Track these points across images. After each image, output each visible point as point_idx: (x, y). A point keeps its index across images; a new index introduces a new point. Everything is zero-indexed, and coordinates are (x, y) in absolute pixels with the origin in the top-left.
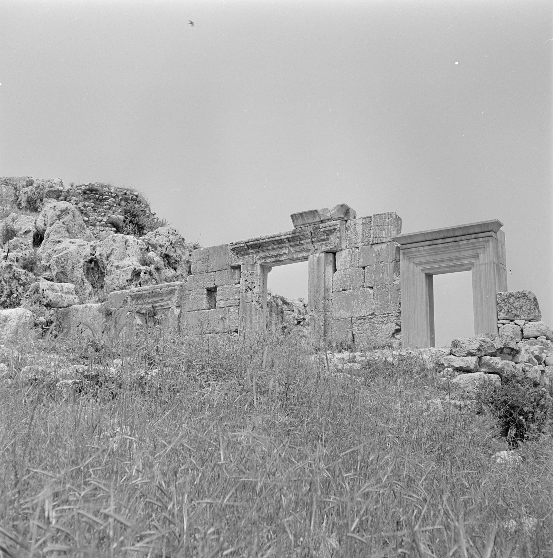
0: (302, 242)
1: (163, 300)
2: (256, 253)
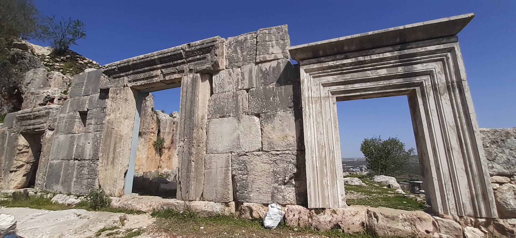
0: (176, 62)
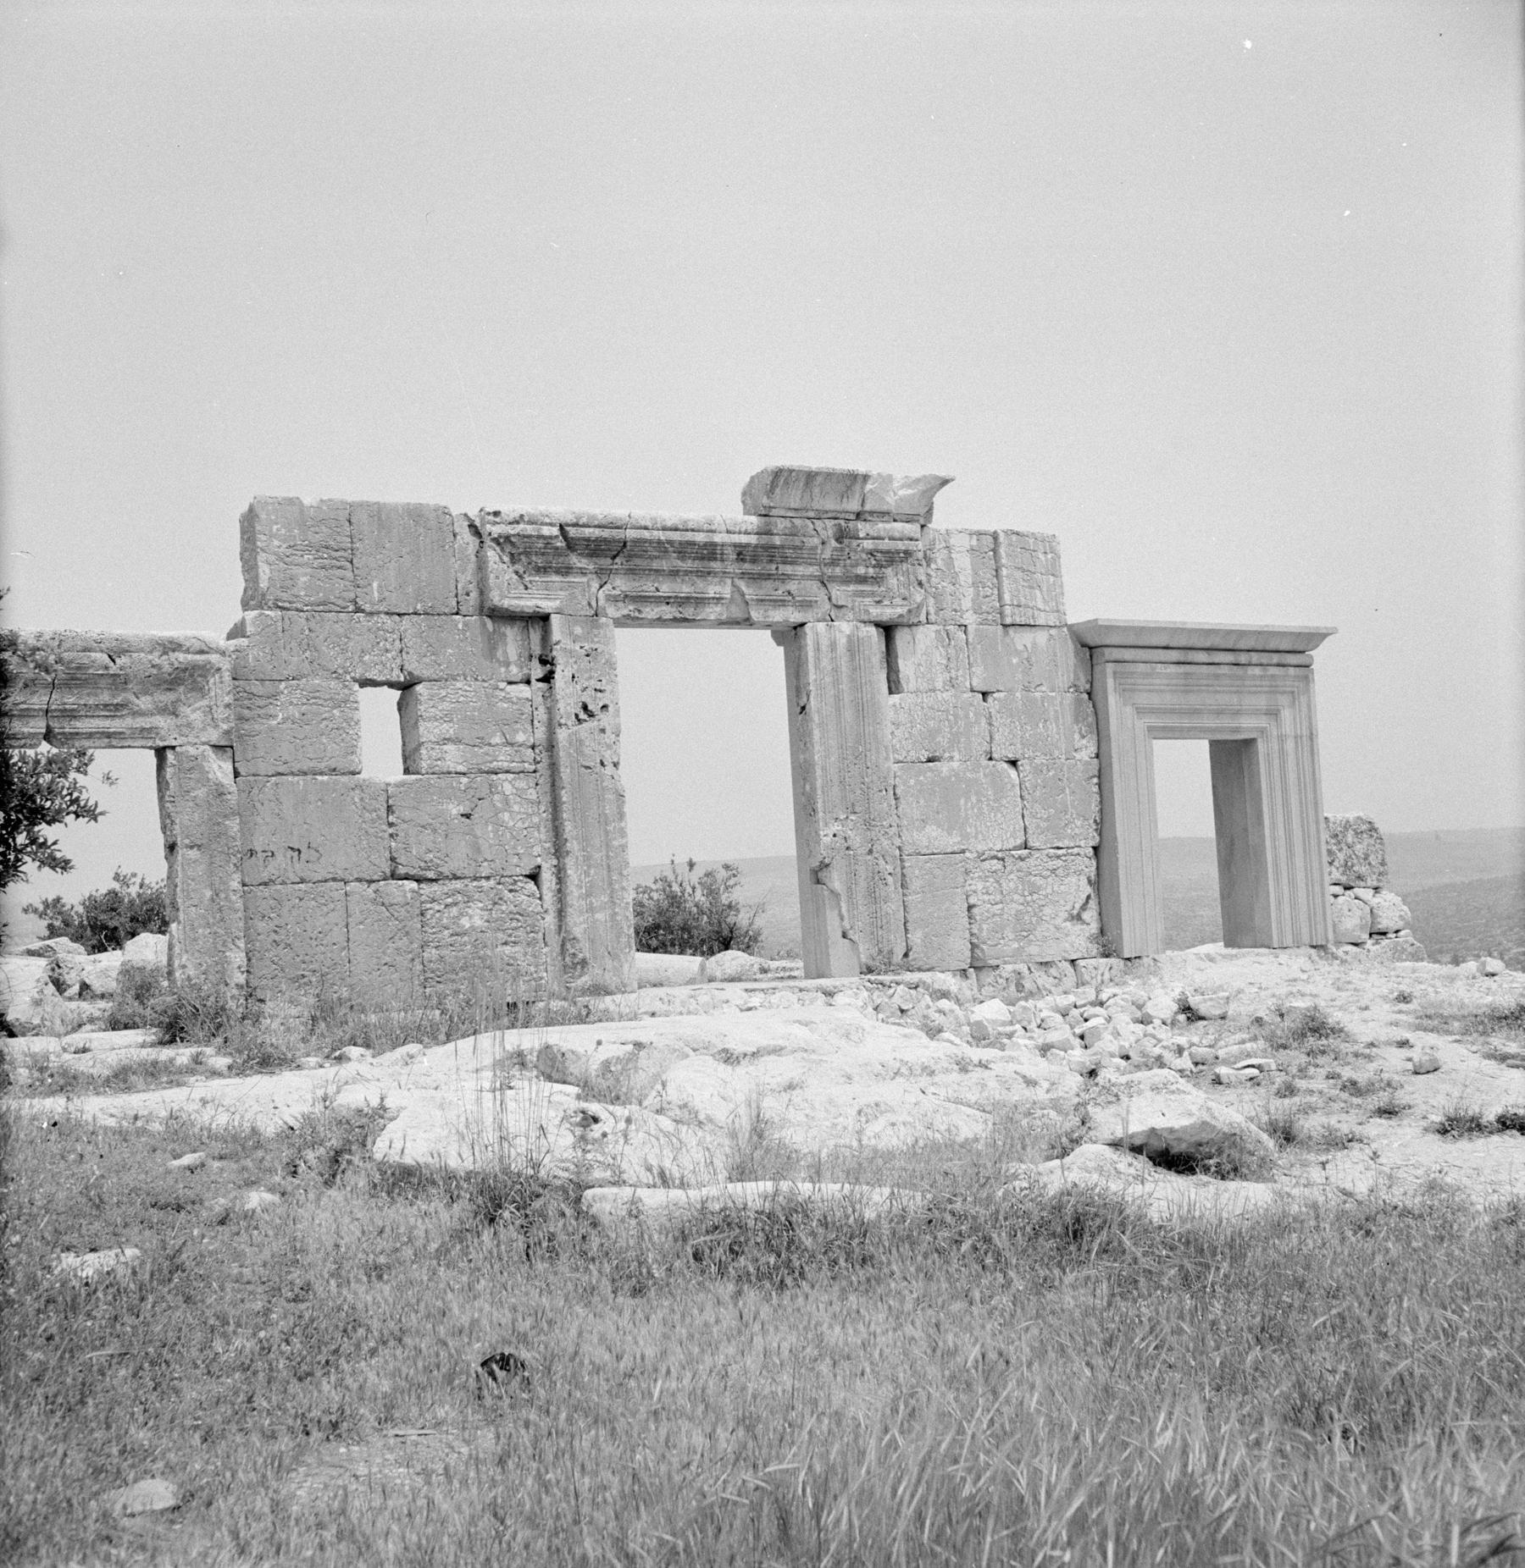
0: (788, 569)
1: (118, 707)
2: (599, 572)
